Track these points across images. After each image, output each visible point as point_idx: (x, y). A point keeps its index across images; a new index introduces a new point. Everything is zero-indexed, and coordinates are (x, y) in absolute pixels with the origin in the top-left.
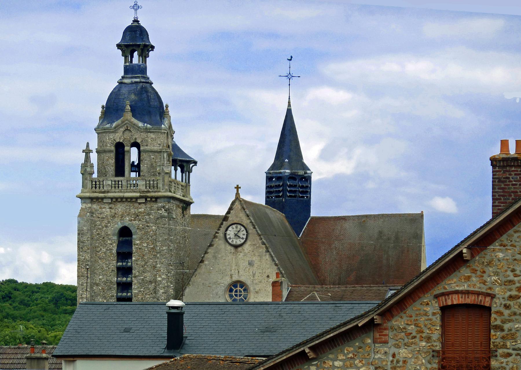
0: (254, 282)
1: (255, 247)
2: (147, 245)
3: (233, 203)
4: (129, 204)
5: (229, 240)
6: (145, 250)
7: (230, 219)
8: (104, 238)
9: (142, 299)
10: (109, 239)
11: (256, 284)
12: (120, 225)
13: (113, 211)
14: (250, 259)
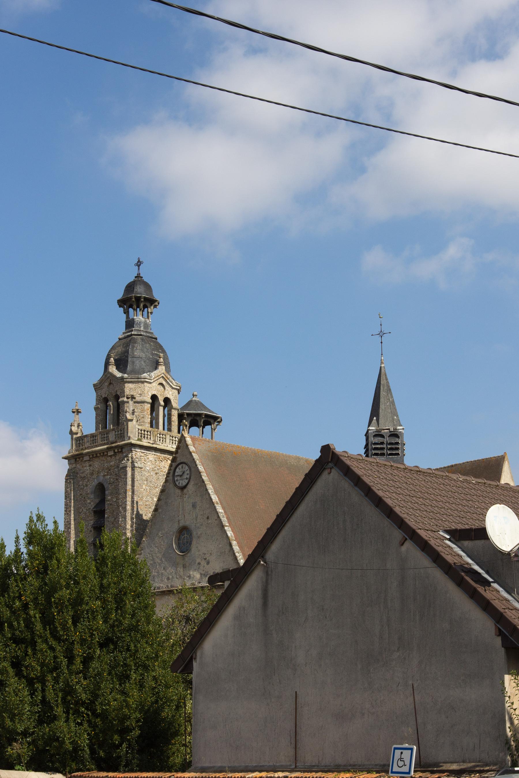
4: (103, 458)
7: (178, 459)
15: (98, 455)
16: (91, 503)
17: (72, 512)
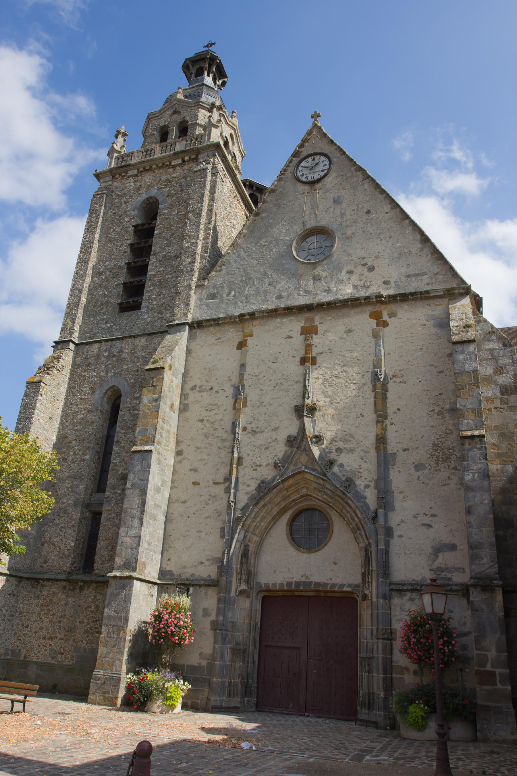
0: (344, 224)
1: (345, 178)
2: (178, 212)
3: (309, 133)
5: (301, 178)
6: (173, 219)
8: (120, 216)
10: (127, 216)
11: (347, 226)
12: (144, 196)
13: (138, 184)
15: (154, 166)
16: (132, 217)
17: (98, 231)
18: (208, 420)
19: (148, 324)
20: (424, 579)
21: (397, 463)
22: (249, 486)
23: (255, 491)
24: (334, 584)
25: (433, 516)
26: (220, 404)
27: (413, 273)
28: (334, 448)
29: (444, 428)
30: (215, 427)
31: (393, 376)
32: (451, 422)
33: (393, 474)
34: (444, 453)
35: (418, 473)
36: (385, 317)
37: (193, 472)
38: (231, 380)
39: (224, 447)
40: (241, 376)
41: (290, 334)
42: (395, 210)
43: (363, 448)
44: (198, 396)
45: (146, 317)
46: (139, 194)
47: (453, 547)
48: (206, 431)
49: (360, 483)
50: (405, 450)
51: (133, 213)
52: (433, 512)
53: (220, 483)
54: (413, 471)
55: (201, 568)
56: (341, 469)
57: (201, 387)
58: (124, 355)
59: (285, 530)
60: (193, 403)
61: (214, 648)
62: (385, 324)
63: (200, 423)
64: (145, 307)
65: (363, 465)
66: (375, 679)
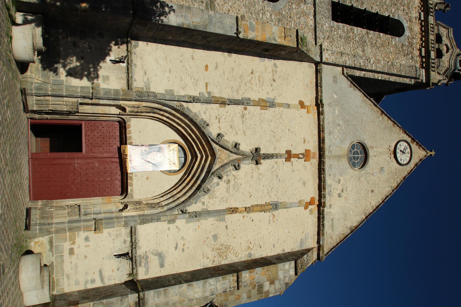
1: (394, 174)
9: (350, 37)
10: (395, 11)
11: (366, 178)
12: (406, 25)
14: (385, 169)
18: (252, 78)
19: (322, 27)
20: (140, 248)
21: (218, 222)
22: (205, 113)
23: (201, 118)
24: (132, 179)
25: (183, 250)
26: (263, 87)
27: (334, 223)
28: (230, 178)
29: (239, 251)
30: (247, 84)
31: (274, 215)
32: (243, 255)
33: (211, 220)
34: (224, 253)
35: (211, 237)
36: (310, 207)
37: (216, 65)
38: (279, 96)
39: (233, 92)
40: (281, 105)
41: (307, 142)
42: (371, 209)
43: (229, 199)
44: (270, 70)
45: (327, 25)
46: (407, 21)
47: (162, 265)
48: (245, 76)
49: (205, 198)
50: (226, 227)
51: (396, 16)
52: (185, 249)
53: (207, 88)
54: (213, 234)
55: (142, 73)
56: (216, 184)
57: (276, 71)
58: (302, 6)
59: (171, 139)
60: (265, 65)
61: (77, 87)
62: (306, 208)
63: (251, 71)
64: (333, 24)
65: (218, 200)
66: (64, 219)
